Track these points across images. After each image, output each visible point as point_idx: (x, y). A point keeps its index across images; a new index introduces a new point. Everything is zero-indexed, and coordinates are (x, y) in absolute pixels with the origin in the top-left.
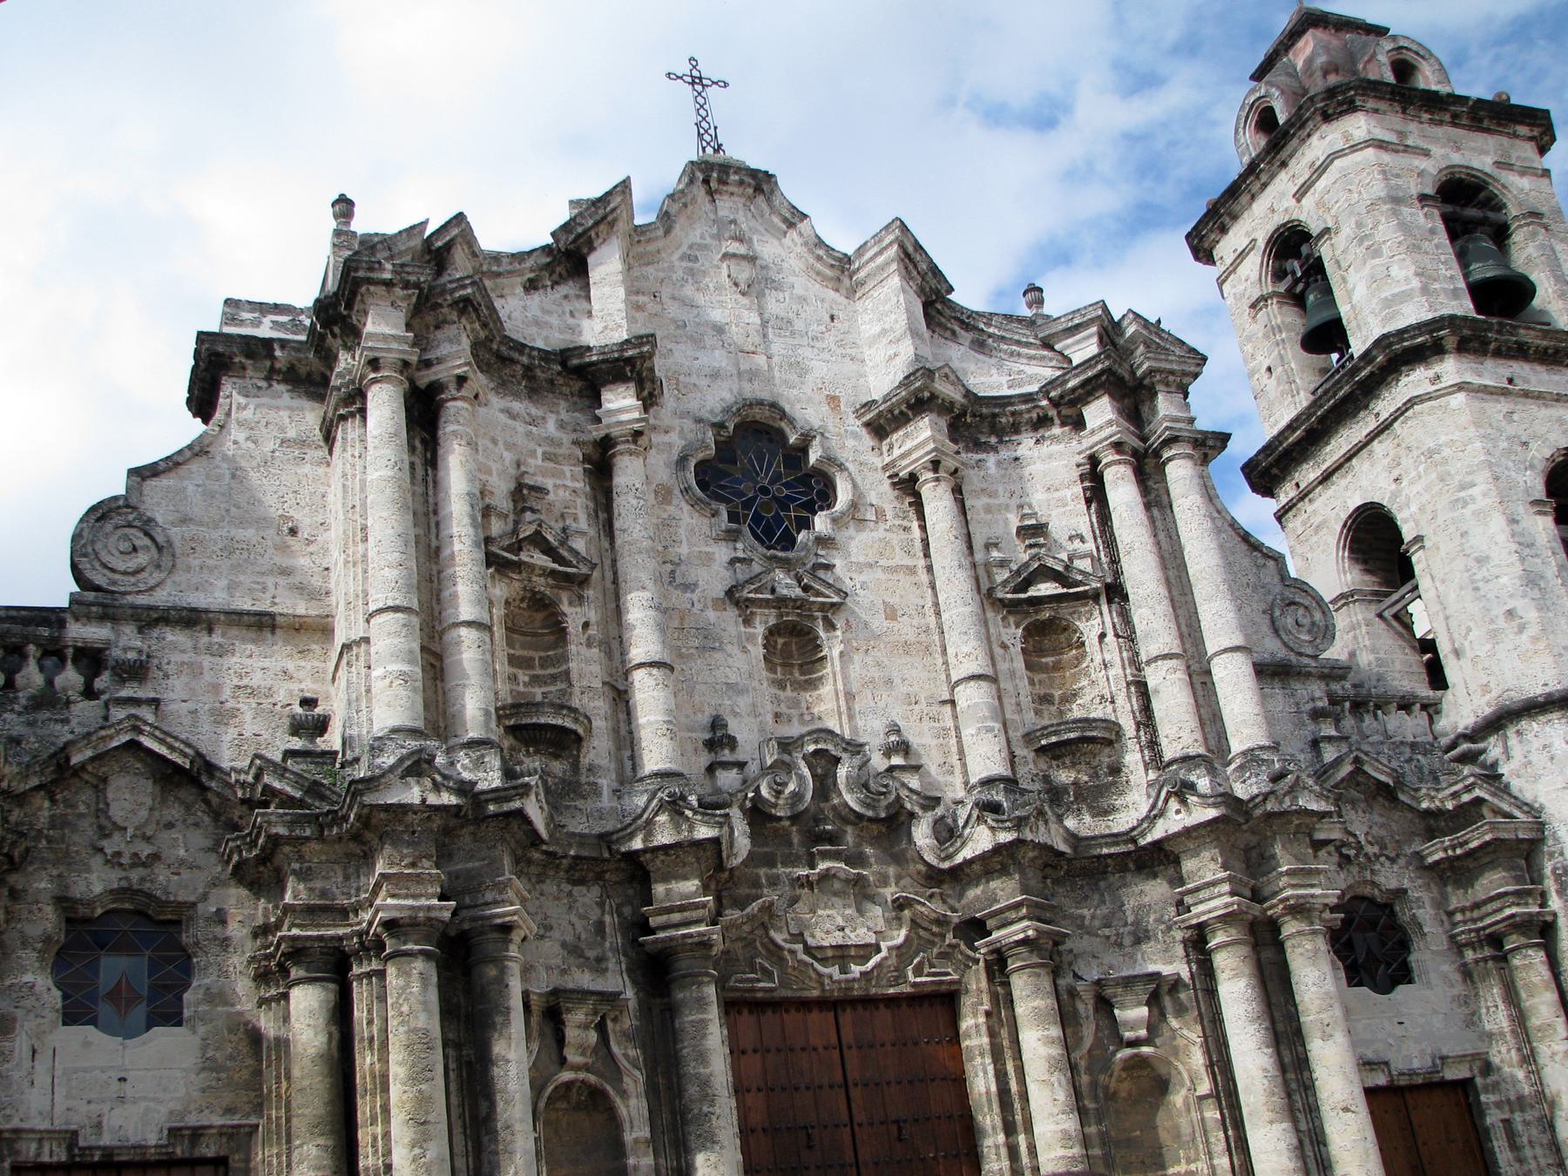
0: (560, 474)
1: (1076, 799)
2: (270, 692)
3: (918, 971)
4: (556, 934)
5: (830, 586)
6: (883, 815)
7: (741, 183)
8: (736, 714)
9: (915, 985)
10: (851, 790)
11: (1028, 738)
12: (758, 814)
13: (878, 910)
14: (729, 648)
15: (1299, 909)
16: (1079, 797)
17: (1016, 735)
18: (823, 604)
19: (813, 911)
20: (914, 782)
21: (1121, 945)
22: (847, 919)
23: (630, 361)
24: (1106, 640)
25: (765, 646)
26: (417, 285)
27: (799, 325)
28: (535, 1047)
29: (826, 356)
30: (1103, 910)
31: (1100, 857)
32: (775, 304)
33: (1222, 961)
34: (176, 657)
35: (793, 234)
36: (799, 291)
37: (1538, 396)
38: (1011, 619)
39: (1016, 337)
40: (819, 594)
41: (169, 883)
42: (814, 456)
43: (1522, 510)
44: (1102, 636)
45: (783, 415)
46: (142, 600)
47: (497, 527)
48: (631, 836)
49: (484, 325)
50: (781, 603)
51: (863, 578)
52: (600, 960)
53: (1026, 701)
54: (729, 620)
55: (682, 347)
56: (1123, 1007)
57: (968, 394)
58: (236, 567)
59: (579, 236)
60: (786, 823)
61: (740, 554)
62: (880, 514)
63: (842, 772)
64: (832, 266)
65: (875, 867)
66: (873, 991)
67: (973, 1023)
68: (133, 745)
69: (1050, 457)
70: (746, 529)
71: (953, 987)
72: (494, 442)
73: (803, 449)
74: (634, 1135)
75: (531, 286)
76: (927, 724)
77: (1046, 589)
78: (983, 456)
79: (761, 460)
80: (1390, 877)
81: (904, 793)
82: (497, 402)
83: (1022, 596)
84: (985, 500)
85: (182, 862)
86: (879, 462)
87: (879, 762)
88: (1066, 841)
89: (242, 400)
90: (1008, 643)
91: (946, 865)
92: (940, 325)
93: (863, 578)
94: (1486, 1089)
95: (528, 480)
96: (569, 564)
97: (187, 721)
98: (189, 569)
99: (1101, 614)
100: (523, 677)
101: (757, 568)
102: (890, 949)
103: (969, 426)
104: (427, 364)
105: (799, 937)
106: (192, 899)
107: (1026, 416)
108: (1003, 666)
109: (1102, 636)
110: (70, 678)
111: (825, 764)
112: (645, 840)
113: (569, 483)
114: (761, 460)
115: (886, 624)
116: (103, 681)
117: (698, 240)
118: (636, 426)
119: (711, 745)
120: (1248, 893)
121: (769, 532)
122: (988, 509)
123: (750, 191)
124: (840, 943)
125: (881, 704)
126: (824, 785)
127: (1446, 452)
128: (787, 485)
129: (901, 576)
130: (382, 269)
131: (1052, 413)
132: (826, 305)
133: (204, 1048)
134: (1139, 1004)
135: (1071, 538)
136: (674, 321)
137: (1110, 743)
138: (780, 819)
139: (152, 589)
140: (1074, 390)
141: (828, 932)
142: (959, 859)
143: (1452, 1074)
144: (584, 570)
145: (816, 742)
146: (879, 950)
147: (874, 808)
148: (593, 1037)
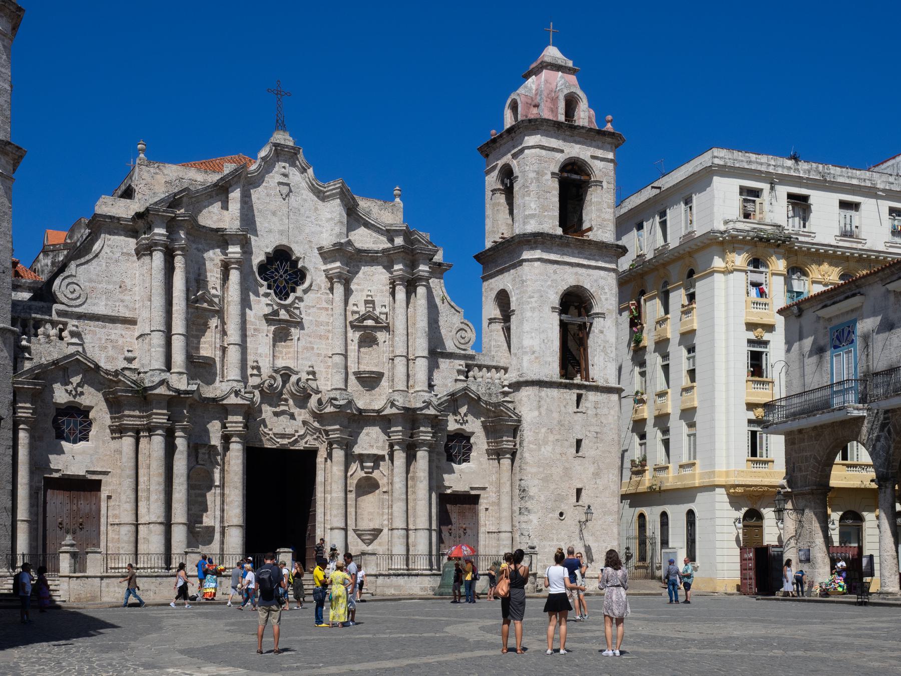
2: (117, 341)
11: (355, 373)
20: (313, 384)
42: (300, 266)
43: (547, 309)
50: (280, 320)
51: (309, 311)
54: (264, 326)
61: (270, 302)
70: (272, 291)
77: (370, 323)
80: (468, 428)
94: (484, 498)
97: (91, 349)
98: (91, 298)
101: (276, 307)
111: (286, 377)
114: (281, 265)
121: (281, 292)
127: (528, 283)
128: (289, 274)
129: (323, 311)
135: (382, 306)
143: (473, 492)
146: (294, 435)
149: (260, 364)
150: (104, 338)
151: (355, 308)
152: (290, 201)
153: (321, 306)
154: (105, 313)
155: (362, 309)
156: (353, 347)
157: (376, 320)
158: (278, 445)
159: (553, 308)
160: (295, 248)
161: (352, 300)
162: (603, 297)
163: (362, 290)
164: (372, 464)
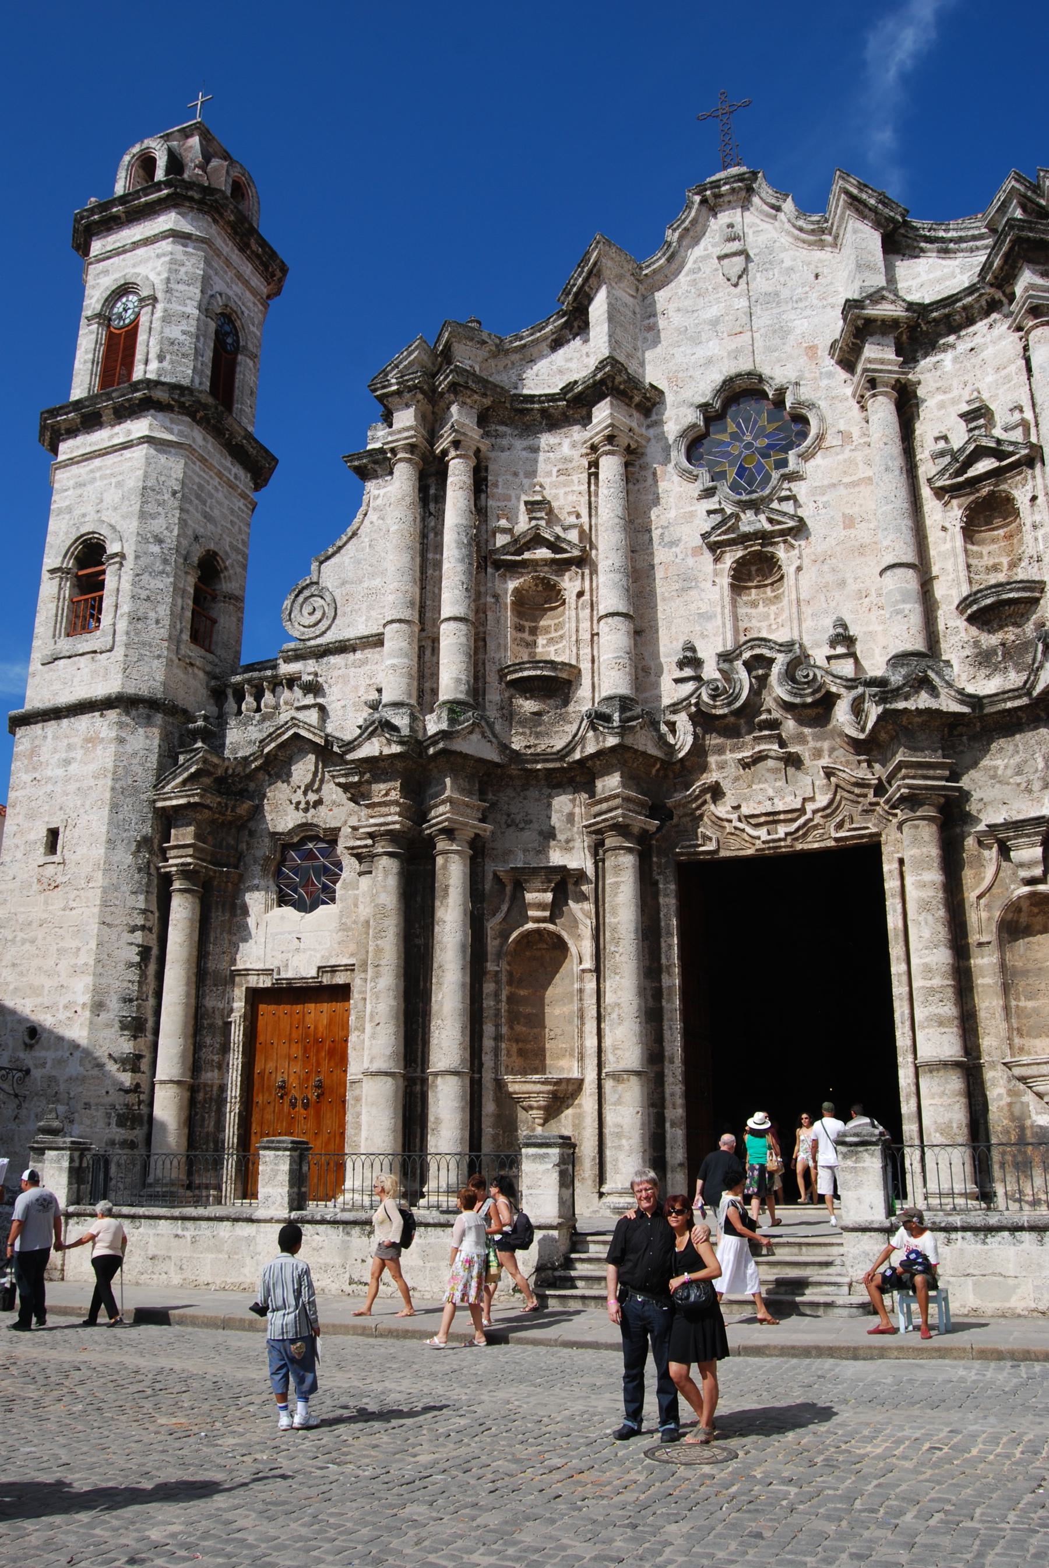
1: (1004, 658)
3: (840, 826)
4: (535, 826)
5: (785, 514)
6: (809, 700)
7: (733, 190)
8: (703, 636)
9: (836, 840)
10: (781, 684)
13: (808, 780)
14: (702, 585)
15: (449, 833)
16: (1007, 655)
18: (782, 530)
19: (750, 786)
21: (1029, 791)
22: (779, 791)
23: (602, 381)
24: (1038, 501)
25: (733, 577)
26: (415, 387)
27: (785, 293)
28: (505, 908)
29: (808, 312)
30: (1017, 759)
31: (1009, 710)
32: (760, 282)
34: (336, 673)
35: (781, 216)
36: (787, 263)
38: (955, 502)
39: (970, 233)
40: (780, 523)
41: (325, 818)
42: (788, 405)
44: (1034, 498)
45: (761, 379)
46: (319, 641)
48: (574, 749)
49: (484, 395)
50: (744, 539)
51: (825, 499)
52: (568, 841)
55: (682, 349)
56: (1018, 848)
57: (911, 306)
58: (370, 608)
59: (577, 294)
60: (732, 719)
62: (846, 437)
63: (776, 669)
64: (813, 231)
65: (812, 744)
66: (799, 846)
68: (296, 735)
69: (1001, 337)
71: (875, 839)
72: (516, 474)
74: (582, 967)
75: (557, 344)
78: (941, 356)
79: (747, 421)
81: (828, 679)
83: (961, 479)
84: (940, 397)
85: (334, 803)
87: (819, 654)
88: (962, 702)
89: (376, 492)
90: (947, 525)
91: (862, 736)
92: (908, 246)
93: (825, 499)
97: (340, 713)
99: (1034, 477)
102: (815, 812)
103: (927, 333)
105: (737, 807)
106: (338, 825)
107: (977, 306)
109: (1034, 498)
112: (582, 752)
113: (575, 488)
115: (844, 533)
117: (703, 253)
118: (606, 432)
119: (681, 664)
122: (941, 406)
123: (743, 194)
124: (770, 810)
125: (833, 604)
126: (762, 682)
128: (767, 436)
129: (862, 488)
130: (391, 385)
131: (999, 295)
132: (812, 267)
133: (341, 917)
134: (1033, 845)
136: (677, 329)
137: (1036, 601)
138: (724, 716)
139: (324, 632)
140: (1001, 268)
141: (759, 803)
142: (867, 731)
144: (576, 553)
145: (752, 648)
146: (802, 811)
147: (801, 696)
148: (549, 897)
149: (700, 655)
151: (942, 444)
152: (752, 286)
153: (855, 478)
154: (366, 633)
157: (997, 453)
158: (759, 844)
160: (766, 371)
161: (926, 430)
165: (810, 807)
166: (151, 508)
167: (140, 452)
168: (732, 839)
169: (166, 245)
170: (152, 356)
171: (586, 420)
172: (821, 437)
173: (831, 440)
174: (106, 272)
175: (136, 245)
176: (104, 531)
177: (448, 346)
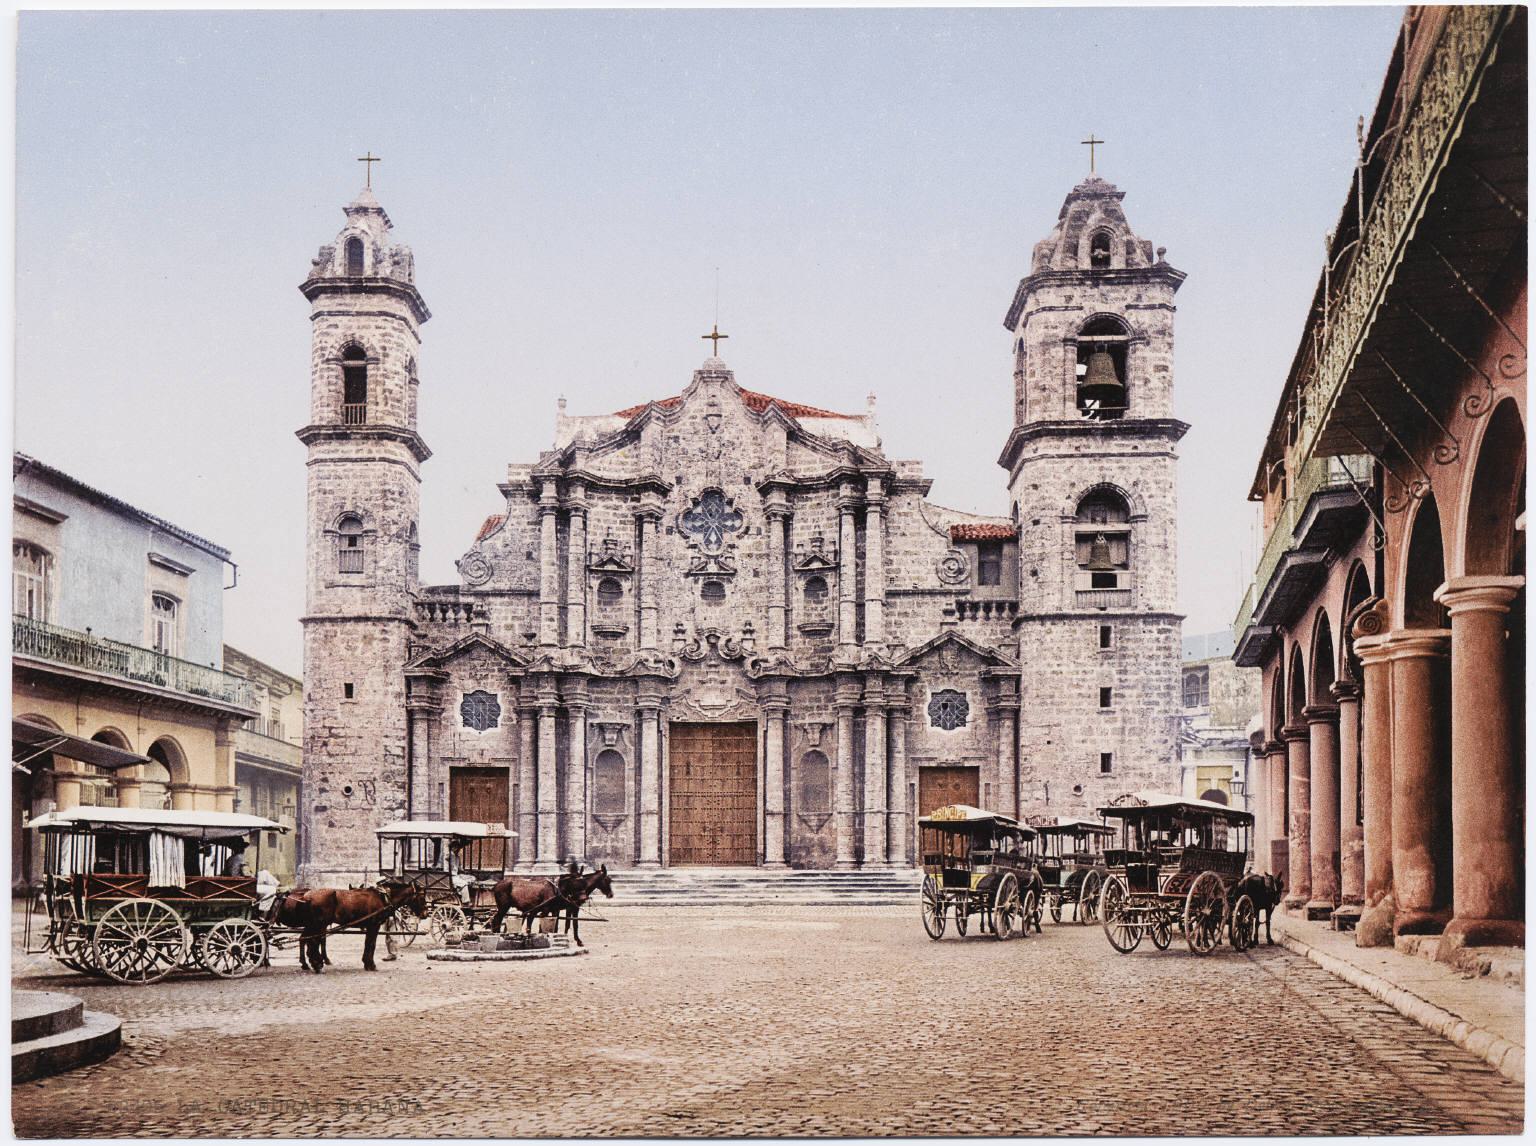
0: (624, 529)
11: (799, 628)
12: (685, 660)
17: (795, 625)
20: (748, 645)
33: (842, 724)
37: (1092, 455)
47: (595, 559)
53: (802, 612)
67: (760, 733)
72: (599, 520)
73: (730, 503)
75: (620, 445)
76: (764, 620)
77: (816, 565)
82: (601, 503)
84: (802, 524)
86: (762, 507)
95: (611, 537)
96: (623, 567)
100: (609, 609)
101: (703, 559)
104: (567, 501)
108: (795, 598)
110: (462, 614)
116: (472, 615)
119: (676, 632)
120: (858, 697)
122: (802, 528)
126: (714, 646)
150: (510, 616)
155: (808, 548)
156: (798, 598)
159: (1062, 518)
162: (1145, 494)
163: (809, 528)
164: (817, 736)
165: (730, 704)
166: (390, 503)
167: (379, 467)
168: (695, 716)
169: (380, 321)
170: (380, 399)
171: (638, 500)
172: (748, 528)
173: (753, 531)
174: (336, 326)
175: (359, 314)
176: (360, 512)
177: (574, 451)
